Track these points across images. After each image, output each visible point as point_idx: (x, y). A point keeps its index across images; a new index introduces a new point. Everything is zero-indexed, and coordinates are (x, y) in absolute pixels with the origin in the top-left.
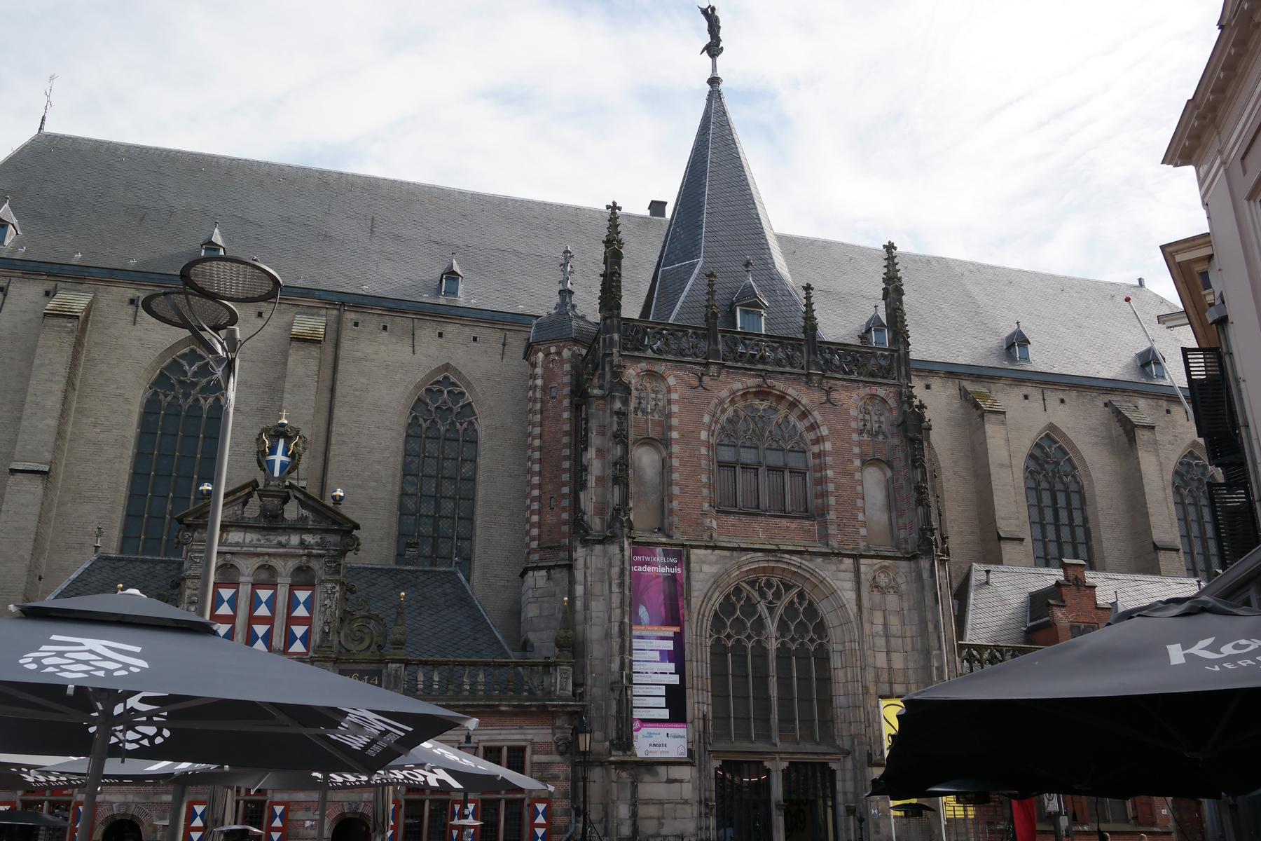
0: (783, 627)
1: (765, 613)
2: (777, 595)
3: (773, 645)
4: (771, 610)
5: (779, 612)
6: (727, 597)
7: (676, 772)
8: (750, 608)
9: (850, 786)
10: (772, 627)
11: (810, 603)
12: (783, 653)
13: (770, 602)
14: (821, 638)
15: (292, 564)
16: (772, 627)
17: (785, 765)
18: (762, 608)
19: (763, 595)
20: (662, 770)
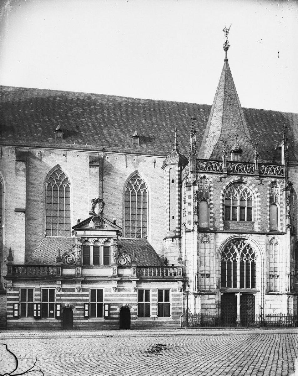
0: (242, 256)
1: (237, 252)
2: (241, 246)
3: (238, 262)
4: (239, 250)
5: (241, 251)
6: (226, 247)
7: (211, 296)
8: (233, 250)
9: (260, 301)
10: (238, 256)
11: (251, 248)
12: (242, 263)
13: (239, 248)
14: (253, 259)
15: (104, 240)
16: (238, 256)
17: (241, 294)
18: (236, 250)
19: (237, 246)
20: (207, 296)
